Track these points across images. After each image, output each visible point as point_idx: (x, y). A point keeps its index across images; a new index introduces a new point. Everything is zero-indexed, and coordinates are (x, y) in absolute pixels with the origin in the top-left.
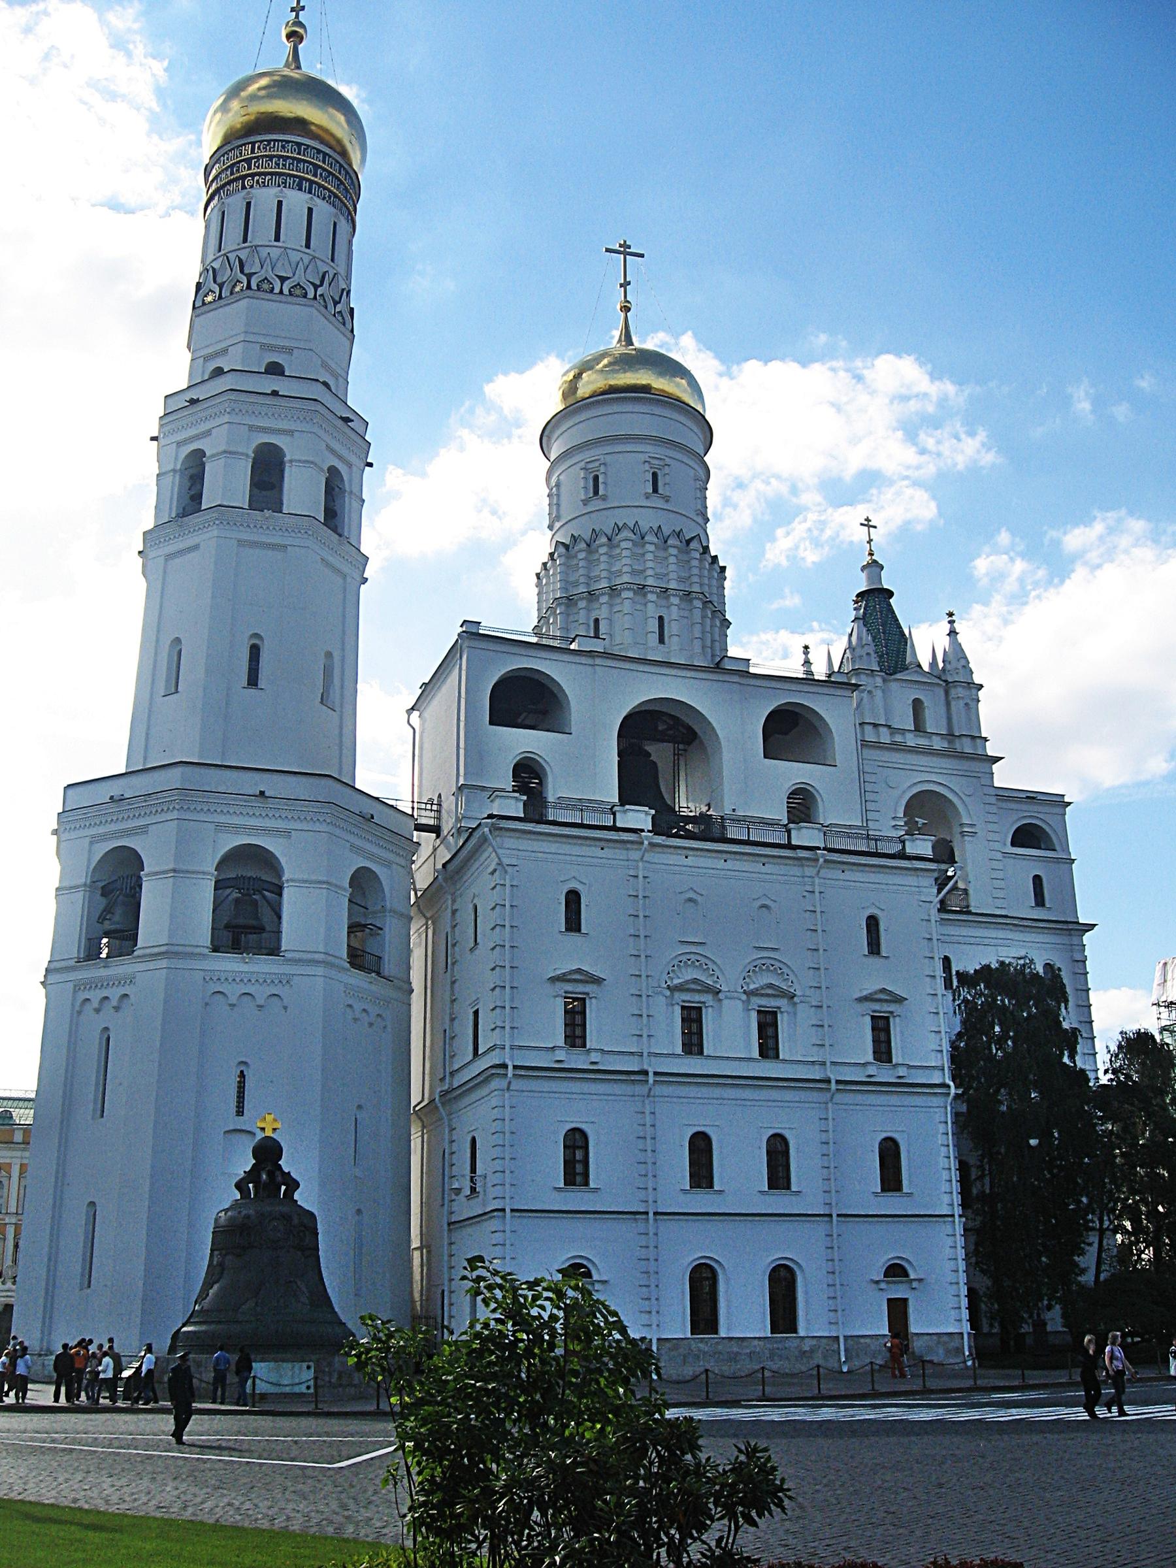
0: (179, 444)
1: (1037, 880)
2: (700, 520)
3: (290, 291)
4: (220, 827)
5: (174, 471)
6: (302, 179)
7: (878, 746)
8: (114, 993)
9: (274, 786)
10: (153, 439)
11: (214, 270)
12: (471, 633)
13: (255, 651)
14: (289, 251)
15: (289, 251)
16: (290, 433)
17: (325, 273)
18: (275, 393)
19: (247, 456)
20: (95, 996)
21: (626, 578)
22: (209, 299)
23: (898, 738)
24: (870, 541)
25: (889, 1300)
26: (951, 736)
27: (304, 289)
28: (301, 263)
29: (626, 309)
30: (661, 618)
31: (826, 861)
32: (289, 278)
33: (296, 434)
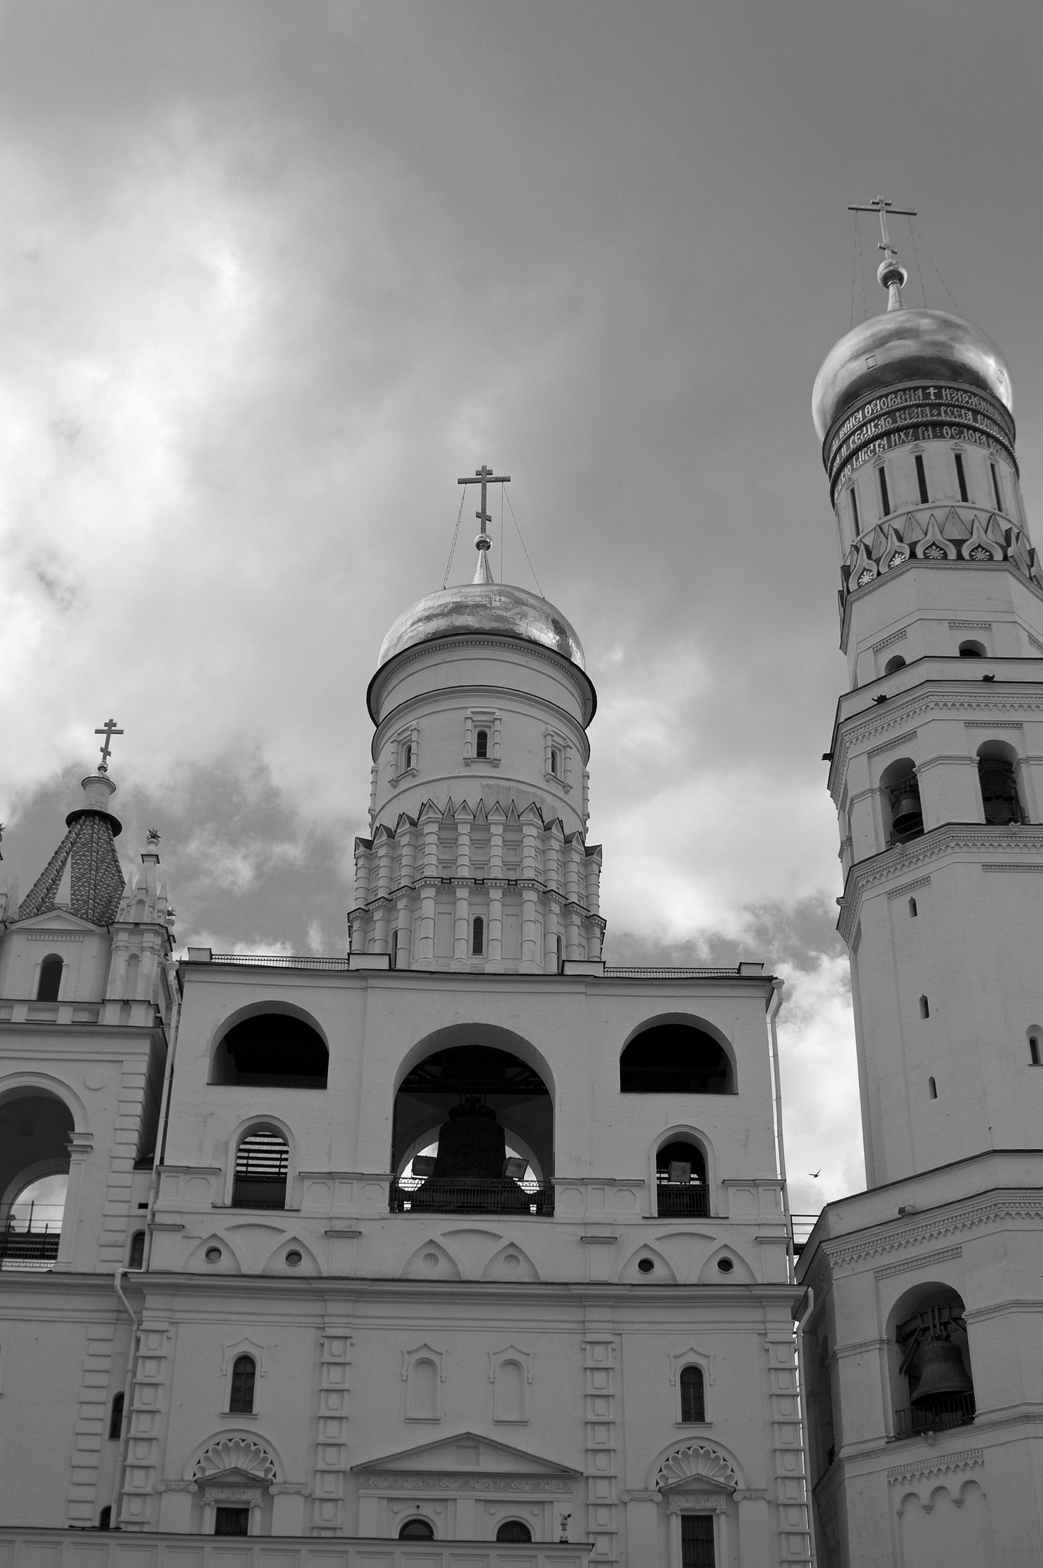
3: (971, 556)
5: (872, 791)
8: (953, 1482)
10: (826, 757)
11: (867, 547)
14: (957, 509)
15: (957, 509)
16: (1018, 725)
17: (1008, 532)
18: (988, 679)
19: (970, 759)
20: (924, 1489)
22: (866, 579)
27: (987, 551)
28: (976, 522)
32: (967, 540)
33: (1025, 725)
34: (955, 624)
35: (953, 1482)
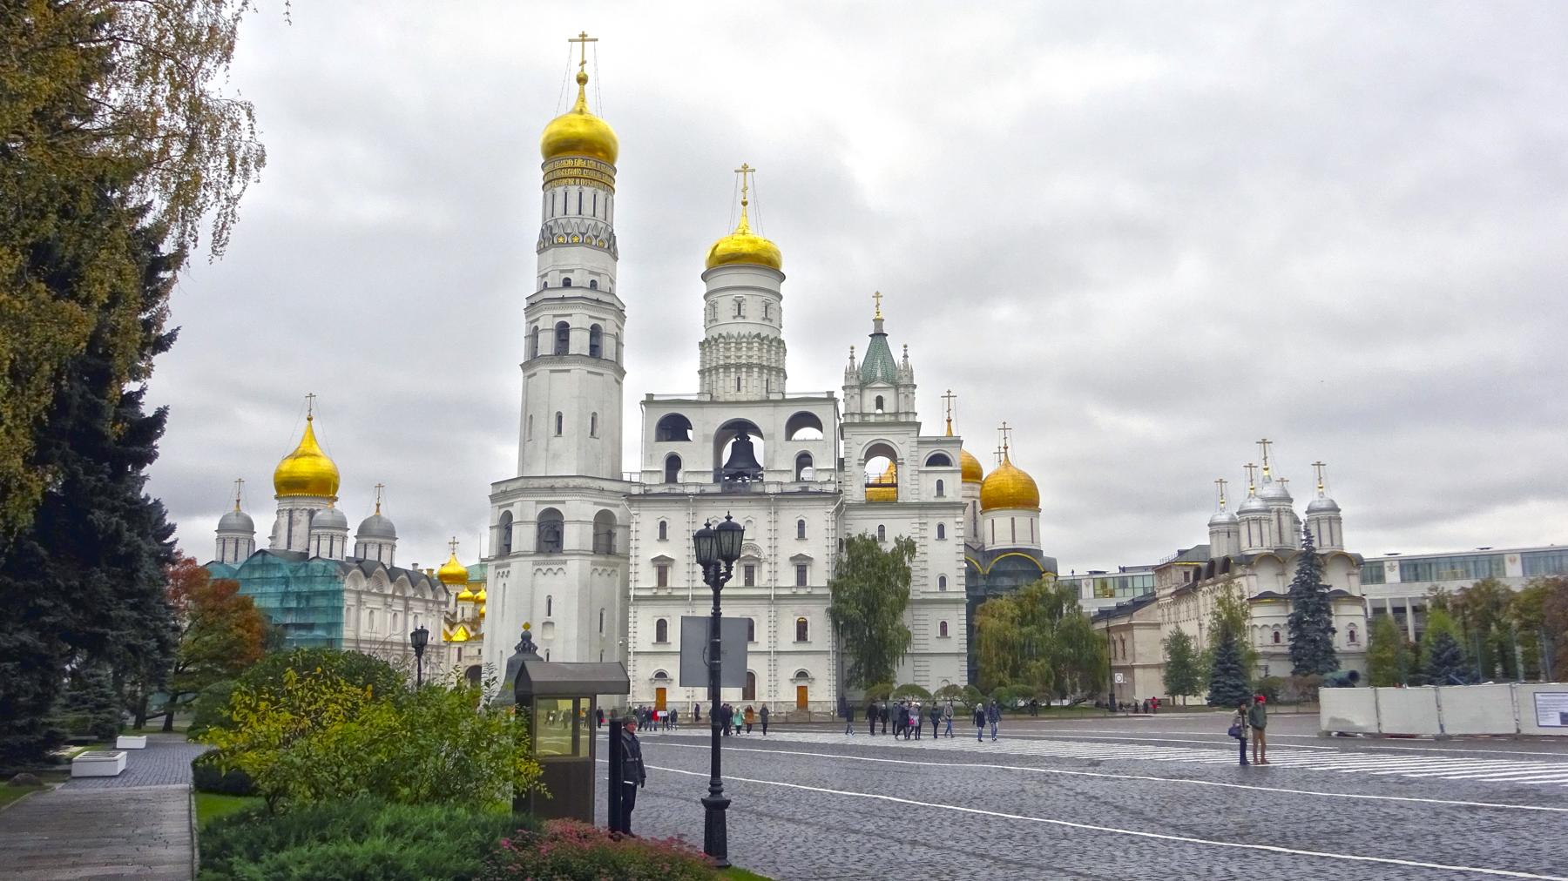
0: (532, 322)
1: (940, 484)
2: (767, 323)
4: (538, 502)
6: (575, 178)
7: (853, 425)
9: (559, 483)
12: (649, 401)
13: (560, 417)
20: (501, 571)
21: (721, 362)
23: (866, 419)
24: (878, 305)
25: (798, 688)
26: (897, 414)
29: (745, 204)
30: (739, 378)
31: (775, 499)
34: (562, 271)
35: (506, 570)
